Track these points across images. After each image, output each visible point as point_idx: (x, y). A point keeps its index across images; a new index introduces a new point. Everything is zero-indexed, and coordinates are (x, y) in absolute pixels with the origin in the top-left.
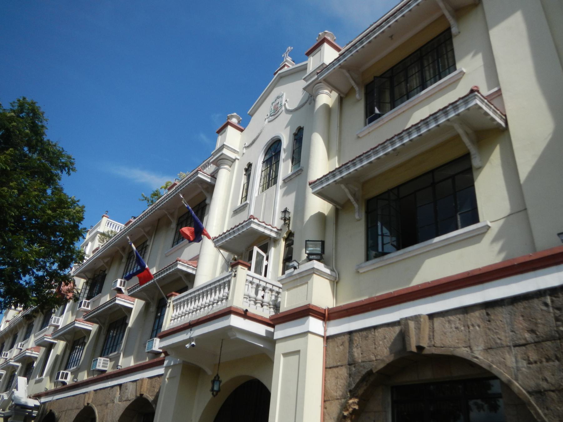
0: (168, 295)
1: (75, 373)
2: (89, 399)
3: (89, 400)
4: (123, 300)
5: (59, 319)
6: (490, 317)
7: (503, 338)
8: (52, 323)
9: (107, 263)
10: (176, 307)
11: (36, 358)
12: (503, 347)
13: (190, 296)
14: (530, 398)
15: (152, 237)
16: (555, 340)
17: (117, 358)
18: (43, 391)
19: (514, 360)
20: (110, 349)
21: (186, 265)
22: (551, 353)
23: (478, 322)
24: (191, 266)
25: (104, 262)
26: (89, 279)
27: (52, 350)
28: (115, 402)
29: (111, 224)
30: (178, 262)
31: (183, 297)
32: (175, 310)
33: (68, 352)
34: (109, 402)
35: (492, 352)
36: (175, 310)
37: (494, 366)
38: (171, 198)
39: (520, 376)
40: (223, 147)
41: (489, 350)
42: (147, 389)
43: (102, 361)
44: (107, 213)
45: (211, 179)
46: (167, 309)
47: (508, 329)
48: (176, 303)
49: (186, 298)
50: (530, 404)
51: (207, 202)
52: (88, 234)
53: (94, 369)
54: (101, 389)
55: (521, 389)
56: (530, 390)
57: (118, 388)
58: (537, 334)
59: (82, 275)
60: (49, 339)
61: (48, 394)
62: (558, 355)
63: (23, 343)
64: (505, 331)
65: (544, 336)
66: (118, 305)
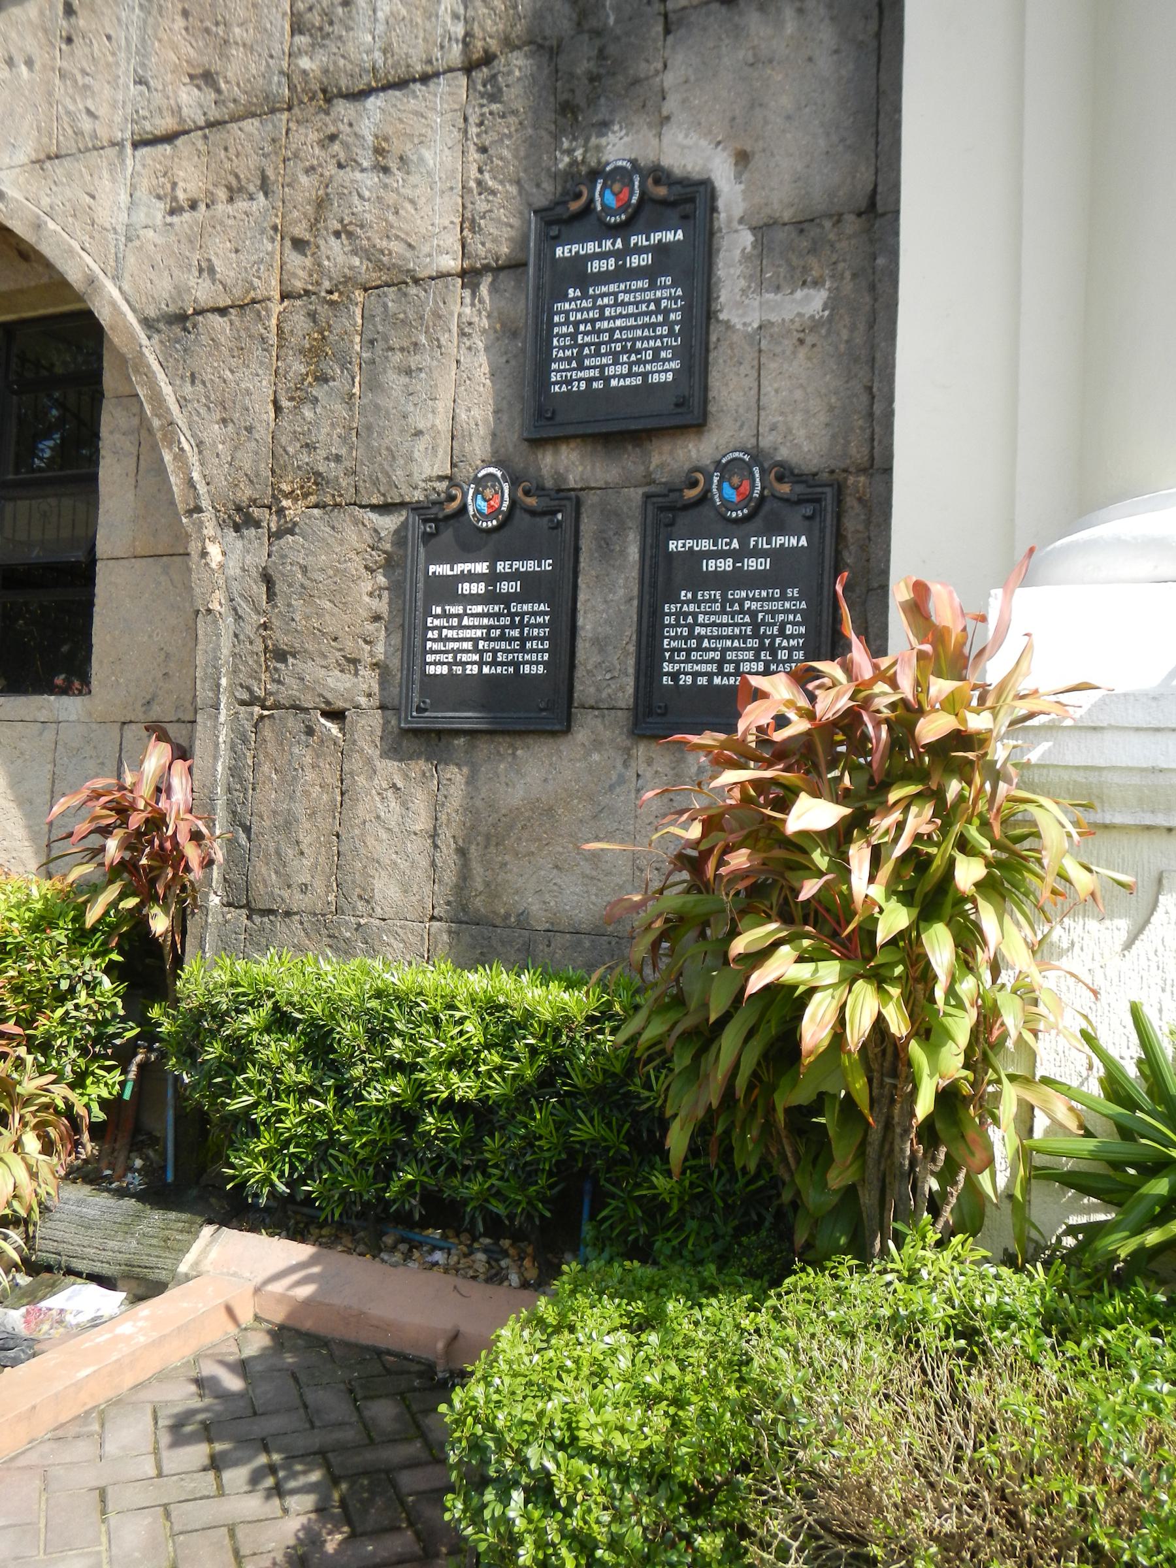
6: (73, 20)
7: (102, 112)
12: (95, 148)
14: (145, 341)
16: (273, 111)
19: (124, 198)
22: (247, 167)
23: (31, 45)
35: (57, 169)
37: (51, 225)
39: (131, 260)
41: (48, 165)
47: (125, 71)
50: (140, 363)
55: (125, 308)
56: (152, 312)
58: (218, 91)
62: (270, 173)
64: (114, 83)
65: (243, 99)
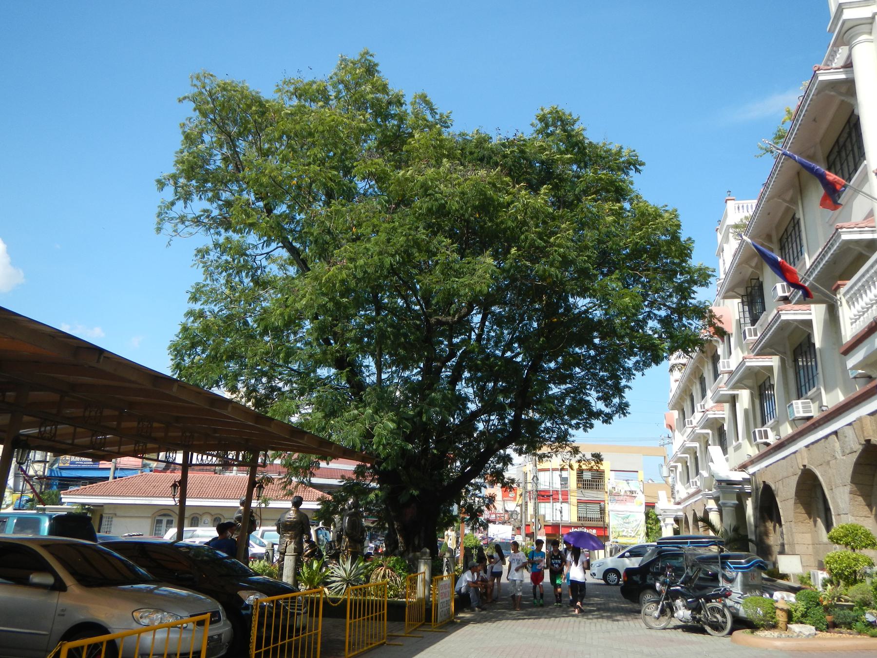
0: (833, 288)
1: (775, 428)
2: (802, 459)
3: (804, 460)
4: (792, 312)
5: (728, 362)
8: (722, 369)
9: (756, 267)
10: (851, 302)
11: (724, 419)
13: (864, 280)
15: (797, 205)
17: (817, 398)
18: (746, 459)
20: (807, 385)
21: (856, 229)
24: (867, 229)
25: (752, 267)
26: (742, 296)
27: (737, 405)
28: (838, 457)
29: (743, 206)
30: (839, 230)
31: (855, 284)
32: (852, 307)
33: (757, 402)
34: (829, 458)
36: (852, 307)
38: (796, 134)
40: (840, 8)
42: (874, 431)
43: (800, 405)
44: (729, 195)
45: (846, 72)
46: (840, 309)
48: (848, 296)
49: (860, 284)
51: (856, 112)
52: (718, 233)
53: (793, 417)
54: (813, 443)
57: (834, 437)
59: (731, 293)
60: (726, 391)
61: (753, 461)
63: (702, 403)
66: (787, 323)
